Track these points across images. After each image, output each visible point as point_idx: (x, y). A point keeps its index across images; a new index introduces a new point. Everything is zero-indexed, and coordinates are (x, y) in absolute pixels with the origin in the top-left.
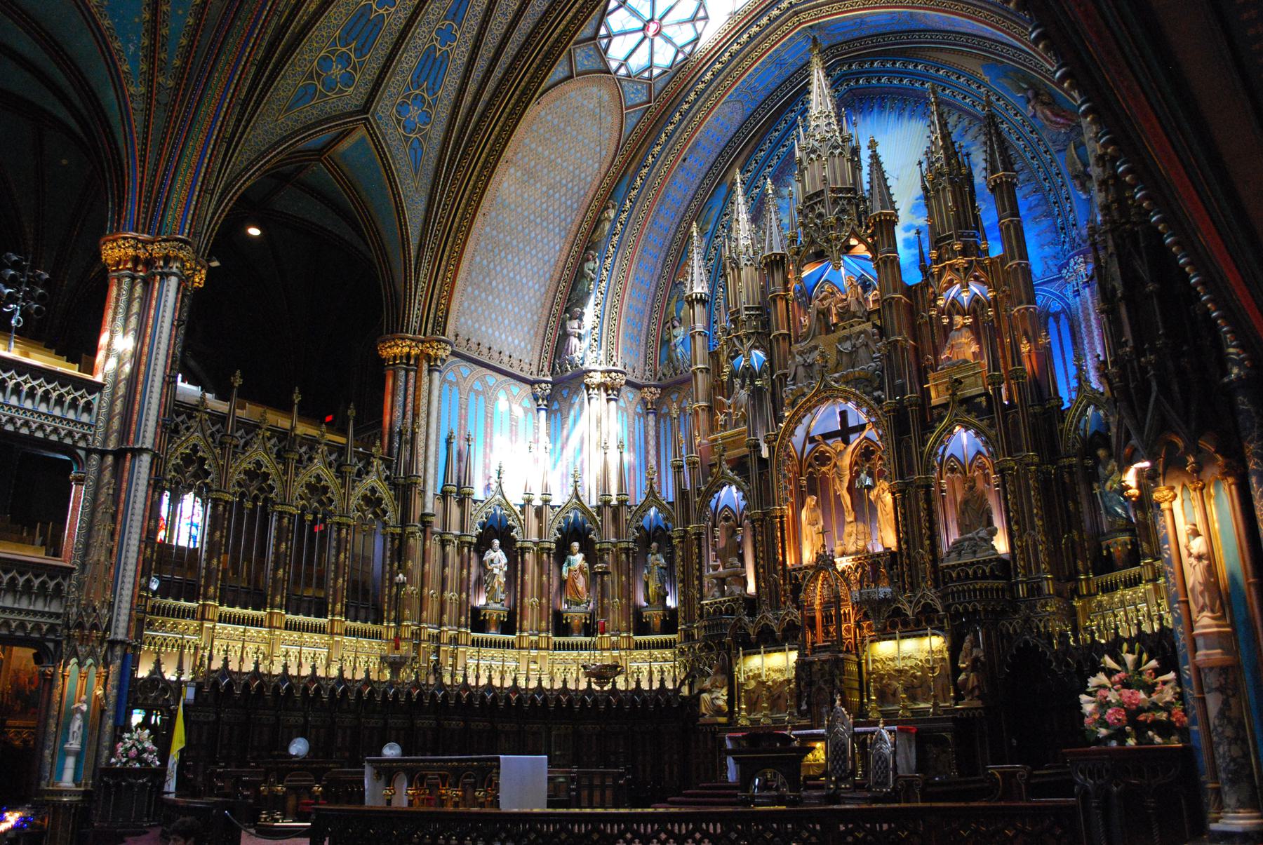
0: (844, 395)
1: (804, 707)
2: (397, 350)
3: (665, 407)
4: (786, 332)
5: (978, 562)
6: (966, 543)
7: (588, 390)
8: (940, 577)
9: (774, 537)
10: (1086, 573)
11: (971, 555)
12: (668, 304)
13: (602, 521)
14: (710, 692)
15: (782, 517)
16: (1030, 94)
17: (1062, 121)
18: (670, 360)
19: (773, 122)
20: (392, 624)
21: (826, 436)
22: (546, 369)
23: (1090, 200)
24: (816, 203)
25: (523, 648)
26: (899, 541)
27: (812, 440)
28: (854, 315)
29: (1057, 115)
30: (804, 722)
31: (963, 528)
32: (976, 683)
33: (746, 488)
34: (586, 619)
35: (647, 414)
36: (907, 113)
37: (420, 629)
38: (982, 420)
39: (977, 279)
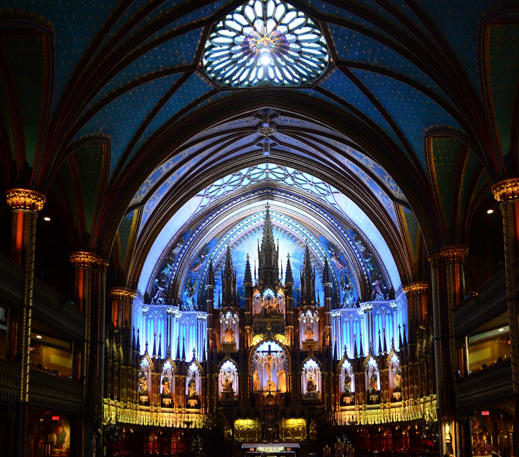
1: (265, 437)
3: (183, 321)
8: (304, 403)
10: (338, 406)
12: (187, 280)
16: (333, 253)
17: (342, 266)
19: (239, 222)
20: (122, 403)
21: (263, 352)
22: (147, 301)
27: (258, 352)
28: (277, 315)
29: (340, 264)
30: (265, 441)
31: (309, 389)
34: (169, 402)
39: (316, 313)
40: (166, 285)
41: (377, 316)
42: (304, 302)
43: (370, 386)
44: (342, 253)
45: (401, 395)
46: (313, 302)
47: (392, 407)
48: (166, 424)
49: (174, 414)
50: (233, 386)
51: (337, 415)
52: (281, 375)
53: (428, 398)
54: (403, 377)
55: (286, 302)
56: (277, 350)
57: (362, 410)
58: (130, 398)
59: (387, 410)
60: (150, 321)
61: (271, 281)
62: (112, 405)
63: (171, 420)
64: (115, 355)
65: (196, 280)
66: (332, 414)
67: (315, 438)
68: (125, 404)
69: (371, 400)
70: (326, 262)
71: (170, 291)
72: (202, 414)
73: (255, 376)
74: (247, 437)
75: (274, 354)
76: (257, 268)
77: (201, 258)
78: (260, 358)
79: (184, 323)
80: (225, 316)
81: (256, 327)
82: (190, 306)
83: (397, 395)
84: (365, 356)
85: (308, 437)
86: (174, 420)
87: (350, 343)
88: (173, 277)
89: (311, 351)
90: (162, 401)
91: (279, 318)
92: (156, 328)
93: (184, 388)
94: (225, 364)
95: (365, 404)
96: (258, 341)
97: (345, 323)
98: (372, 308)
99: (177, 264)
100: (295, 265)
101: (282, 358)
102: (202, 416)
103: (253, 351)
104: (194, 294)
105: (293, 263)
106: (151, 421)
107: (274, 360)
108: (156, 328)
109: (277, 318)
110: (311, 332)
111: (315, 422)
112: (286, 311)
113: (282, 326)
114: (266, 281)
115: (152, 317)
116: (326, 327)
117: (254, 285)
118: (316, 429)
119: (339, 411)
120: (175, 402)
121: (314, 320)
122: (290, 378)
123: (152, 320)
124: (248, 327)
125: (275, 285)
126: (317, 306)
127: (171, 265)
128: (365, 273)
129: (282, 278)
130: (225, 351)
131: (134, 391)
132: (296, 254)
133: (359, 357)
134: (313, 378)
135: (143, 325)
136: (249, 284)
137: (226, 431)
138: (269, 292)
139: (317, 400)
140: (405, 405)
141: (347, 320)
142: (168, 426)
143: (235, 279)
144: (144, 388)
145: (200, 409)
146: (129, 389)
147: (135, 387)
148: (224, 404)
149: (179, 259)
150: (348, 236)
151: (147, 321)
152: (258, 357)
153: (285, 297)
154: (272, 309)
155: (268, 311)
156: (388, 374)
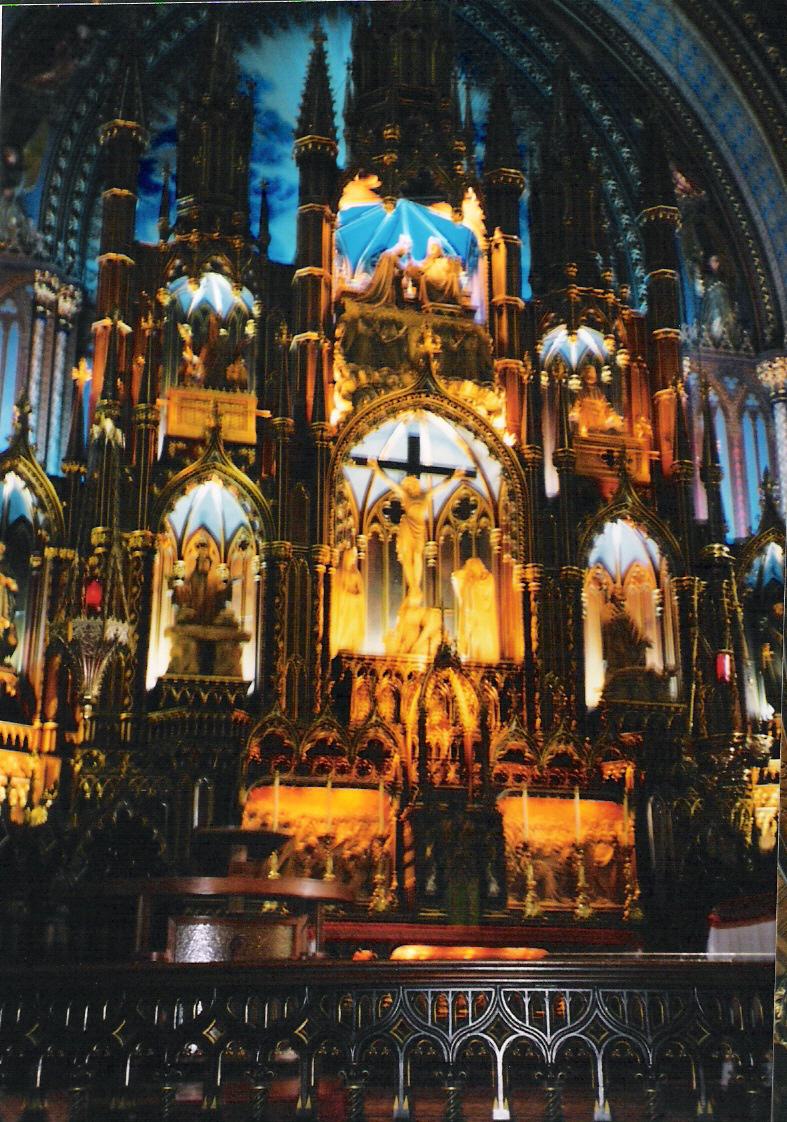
1: (431, 885)
9: (315, 596)
15: (329, 566)
21: (384, 465)
27: (362, 461)
30: (435, 914)
33: (268, 504)
77: (76, 35)
102: (33, 763)
112: (490, 300)
145: (31, 723)
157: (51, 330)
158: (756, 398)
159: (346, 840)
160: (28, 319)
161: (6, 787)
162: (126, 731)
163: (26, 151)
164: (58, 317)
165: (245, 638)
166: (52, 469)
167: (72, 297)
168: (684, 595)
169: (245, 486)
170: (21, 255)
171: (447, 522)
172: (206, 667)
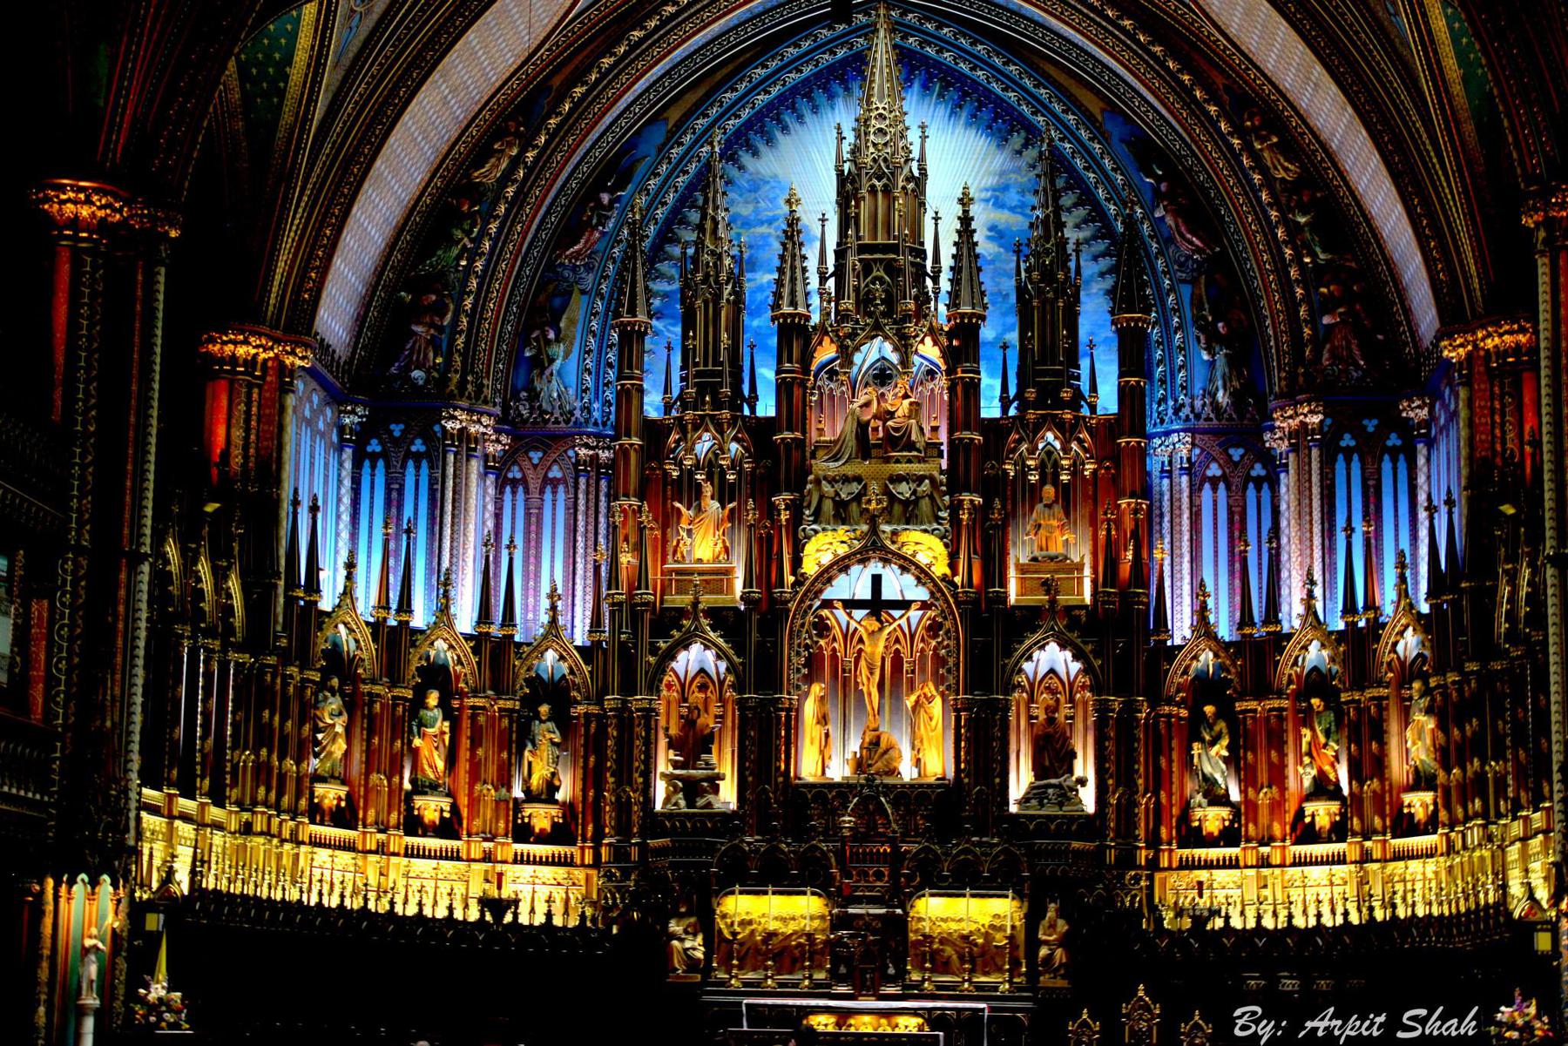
0: (901, 562)
2: (241, 351)
4: (798, 435)
5: (1063, 817)
6: (1050, 791)
7: (445, 438)
9: (778, 736)
11: (1057, 808)
13: (479, 663)
14: (682, 940)
15: (789, 710)
16: (1163, 187)
18: (534, 396)
21: (850, 604)
23: (1212, 364)
24: (875, 260)
25: (370, 852)
26: (958, 770)
27: (828, 604)
30: (842, 989)
31: (1039, 770)
32: (1064, 960)
34: (442, 811)
35: (486, 474)
36: (964, 115)
37: (270, 817)
38: (1085, 643)
39: (1080, 442)
40: (442, 317)
41: (1341, 457)
42: (1031, 393)
43: (1307, 760)
44: (1201, 186)
45: (1435, 803)
46: (1066, 394)
47: (1399, 856)
48: (420, 904)
49: (461, 865)
50: (714, 748)
51: (1164, 883)
52: (921, 706)
53: (1538, 819)
54: (1442, 726)
55: (952, 390)
56: (908, 597)
57: (1270, 866)
58: (268, 791)
59: (1375, 866)
60: (373, 467)
61: (890, 301)
62: (186, 818)
63: (444, 888)
64: (206, 606)
65: (576, 292)
66: (1137, 879)
67: (1061, 983)
68: (246, 816)
69: (1308, 820)
70: (1130, 222)
71: (460, 341)
72: (583, 865)
73: (810, 709)
74: (766, 968)
75: (896, 613)
76: (831, 245)
78: (837, 632)
79: (519, 476)
80: (691, 450)
81: (822, 497)
82: (545, 406)
83: (1419, 803)
84: (1286, 629)
85: (1033, 975)
86: (460, 889)
87: (1231, 573)
88: (474, 283)
89: (1053, 602)
90: (410, 809)
91: (920, 460)
92: (394, 495)
93: (505, 755)
94: (682, 656)
95: (1283, 840)
96: (827, 559)
97: (1207, 486)
98: (1321, 421)
99: (493, 227)
100: (997, 233)
101: (933, 628)
102: (580, 874)
103: (802, 601)
104: (566, 356)
105: (992, 228)
106: (355, 893)
107: (897, 641)
108: (394, 495)
109: (909, 461)
110: (1055, 523)
111: (1061, 913)
112: (951, 432)
113: (931, 497)
114: (864, 301)
115: (378, 449)
116: (1123, 502)
117: (815, 319)
118: (1063, 942)
119: (1170, 868)
120: (465, 812)
121: (1076, 470)
122: (958, 719)
123: (381, 464)
124: (787, 496)
125: (906, 318)
126: (1085, 411)
127: (468, 233)
128: (1294, 273)
129: (937, 292)
130: (682, 600)
131: (289, 763)
132: (1005, 188)
133: (1259, 632)
134: (1060, 716)
135: (340, 481)
136: (792, 316)
137: (675, 943)
138: (877, 350)
139: (1072, 819)
140: (1450, 850)
141: (1219, 473)
142: (428, 912)
143: (738, 294)
144: (334, 748)
145: (573, 843)
146: (264, 752)
147: (293, 745)
148: (673, 825)
149: (502, 209)
150: (1223, 113)
151: (357, 465)
152: (828, 628)
153: (950, 371)
154: (890, 423)
155: (876, 429)
156: (1381, 709)
157: (592, 482)
158: (1264, 467)
159: (795, 933)
160: (571, 482)
161: (548, 901)
162: (634, 853)
163: (562, 325)
164: (599, 466)
165: (721, 777)
166: (578, 642)
167: (609, 448)
168: (1102, 709)
169: (720, 649)
170: (563, 425)
171: (923, 640)
172: (691, 804)
